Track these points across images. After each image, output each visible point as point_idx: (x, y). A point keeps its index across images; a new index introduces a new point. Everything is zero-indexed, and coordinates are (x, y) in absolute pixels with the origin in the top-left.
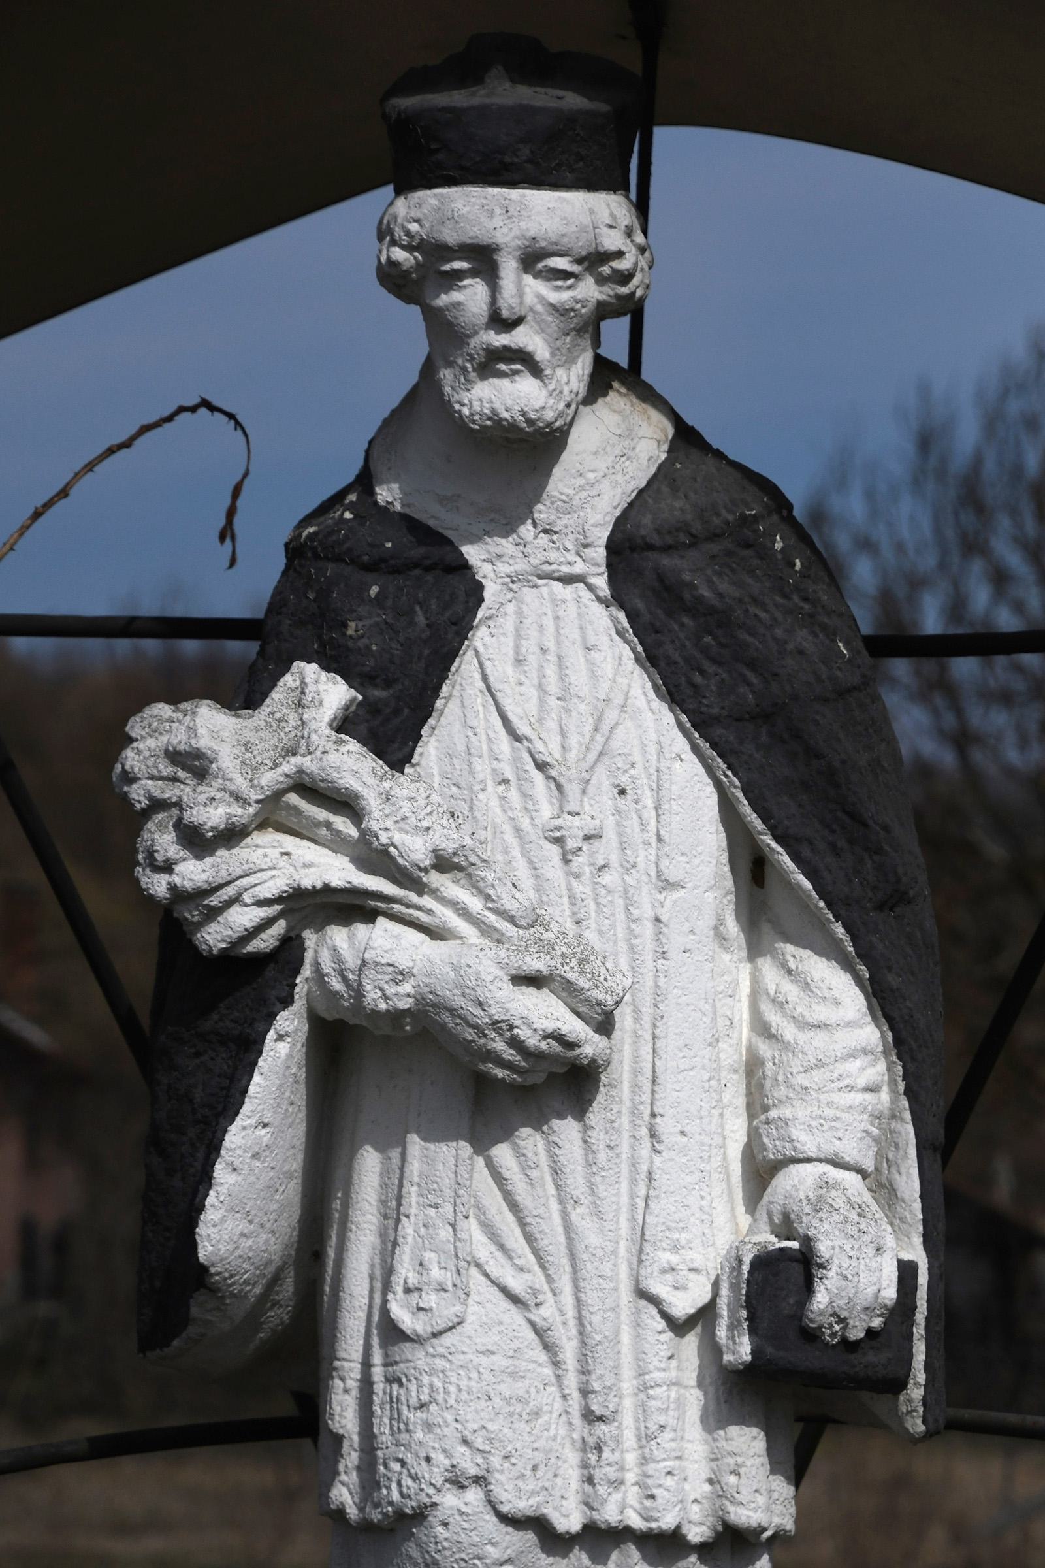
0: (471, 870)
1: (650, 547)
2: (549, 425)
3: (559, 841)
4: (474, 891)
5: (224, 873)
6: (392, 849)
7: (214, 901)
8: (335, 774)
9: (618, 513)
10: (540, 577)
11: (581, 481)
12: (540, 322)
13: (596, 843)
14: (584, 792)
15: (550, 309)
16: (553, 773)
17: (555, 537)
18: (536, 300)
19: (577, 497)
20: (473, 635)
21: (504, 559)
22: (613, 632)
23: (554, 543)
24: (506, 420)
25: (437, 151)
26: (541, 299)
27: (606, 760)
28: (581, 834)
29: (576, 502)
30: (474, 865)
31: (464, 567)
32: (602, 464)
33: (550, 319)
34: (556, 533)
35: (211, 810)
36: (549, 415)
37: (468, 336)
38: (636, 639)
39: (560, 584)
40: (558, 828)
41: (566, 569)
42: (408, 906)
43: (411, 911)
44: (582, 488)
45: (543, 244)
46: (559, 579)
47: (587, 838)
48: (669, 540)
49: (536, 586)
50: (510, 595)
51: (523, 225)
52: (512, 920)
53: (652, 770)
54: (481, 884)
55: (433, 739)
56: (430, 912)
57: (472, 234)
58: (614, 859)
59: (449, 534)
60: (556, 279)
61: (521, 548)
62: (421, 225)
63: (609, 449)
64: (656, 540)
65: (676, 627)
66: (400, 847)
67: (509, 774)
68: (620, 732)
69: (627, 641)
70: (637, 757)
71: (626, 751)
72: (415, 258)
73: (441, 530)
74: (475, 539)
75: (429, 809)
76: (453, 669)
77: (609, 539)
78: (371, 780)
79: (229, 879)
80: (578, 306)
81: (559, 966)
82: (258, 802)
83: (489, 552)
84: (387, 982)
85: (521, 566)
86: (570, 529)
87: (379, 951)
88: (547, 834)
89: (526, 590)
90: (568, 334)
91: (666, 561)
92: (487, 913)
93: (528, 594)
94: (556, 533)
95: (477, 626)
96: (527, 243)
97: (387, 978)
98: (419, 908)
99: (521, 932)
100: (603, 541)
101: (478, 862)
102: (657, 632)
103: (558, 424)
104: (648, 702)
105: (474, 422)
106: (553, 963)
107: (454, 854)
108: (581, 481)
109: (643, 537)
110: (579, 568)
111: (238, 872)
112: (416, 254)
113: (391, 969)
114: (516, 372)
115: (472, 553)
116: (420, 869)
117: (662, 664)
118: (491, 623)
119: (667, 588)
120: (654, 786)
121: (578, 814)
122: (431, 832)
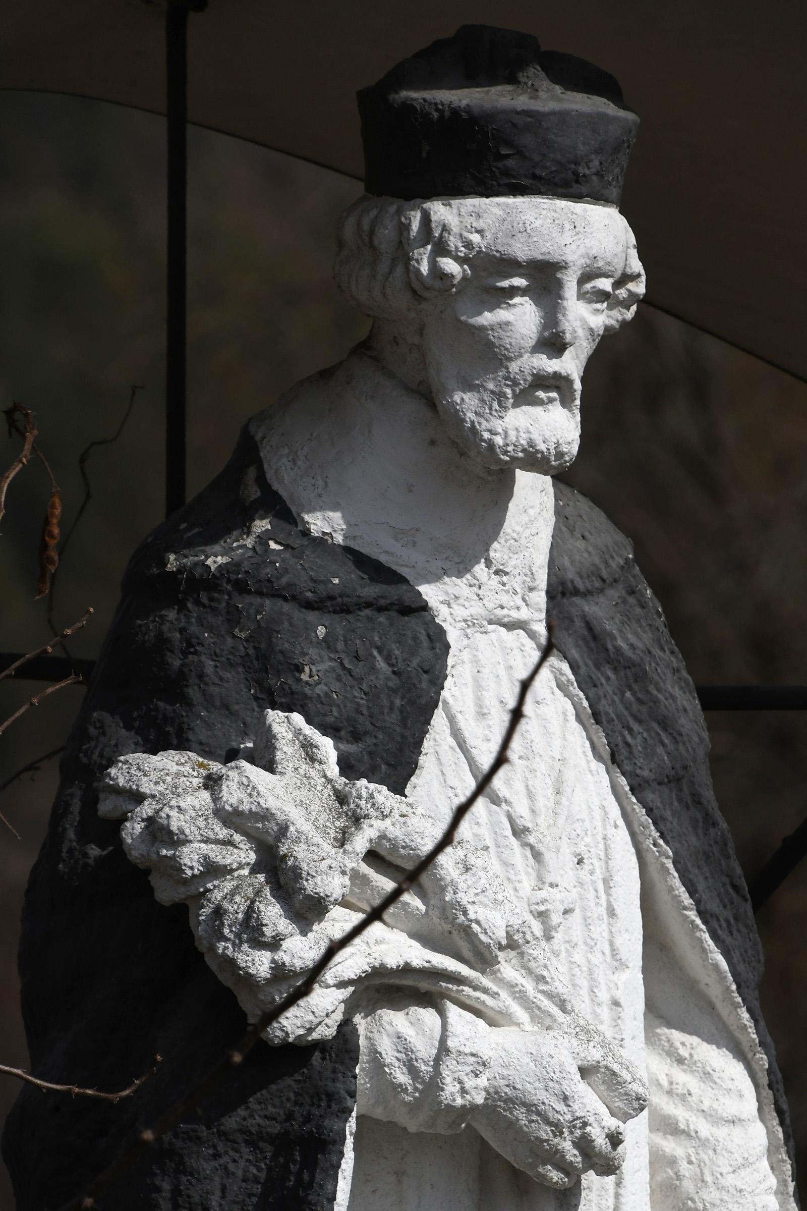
0: (525, 948)
4: (523, 972)
6: (474, 925)
8: (419, 840)
10: (491, 622)
15: (588, 333)
16: (531, 839)
17: (505, 579)
21: (461, 601)
22: (554, 684)
23: (504, 584)
24: (542, 452)
25: (507, 156)
26: (584, 321)
30: (528, 942)
31: (424, 607)
34: (506, 574)
37: (510, 359)
38: (581, 694)
43: (478, 994)
46: (504, 625)
53: (600, 838)
54: (533, 964)
56: (495, 995)
57: (544, 250)
59: (404, 571)
60: (597, 302)
61: (475, 589)
62: (482, 236)
66: (483, 923)
69: (568, 694)
72: (464, 270)
73: (394, 567)
74: (434, 577)
83: (447, 593)
84: (467, 1074)
85: (476, 609)
86: (518, 571)
87: (463, 1041)
88: (533, 907)
89: (478, 635)
92: (540, 996)
94: (506, 574)
96: (588, 262)
97: (468, 1069)
98: (485, 991)
104: (588, 762)
105: (506, 453)
110: (524, 614)
112: (466, 267)
113: (473, 1059)
114: (551, 401)
115: (430, 593)
119: (595, 638)
120: (603, 856)
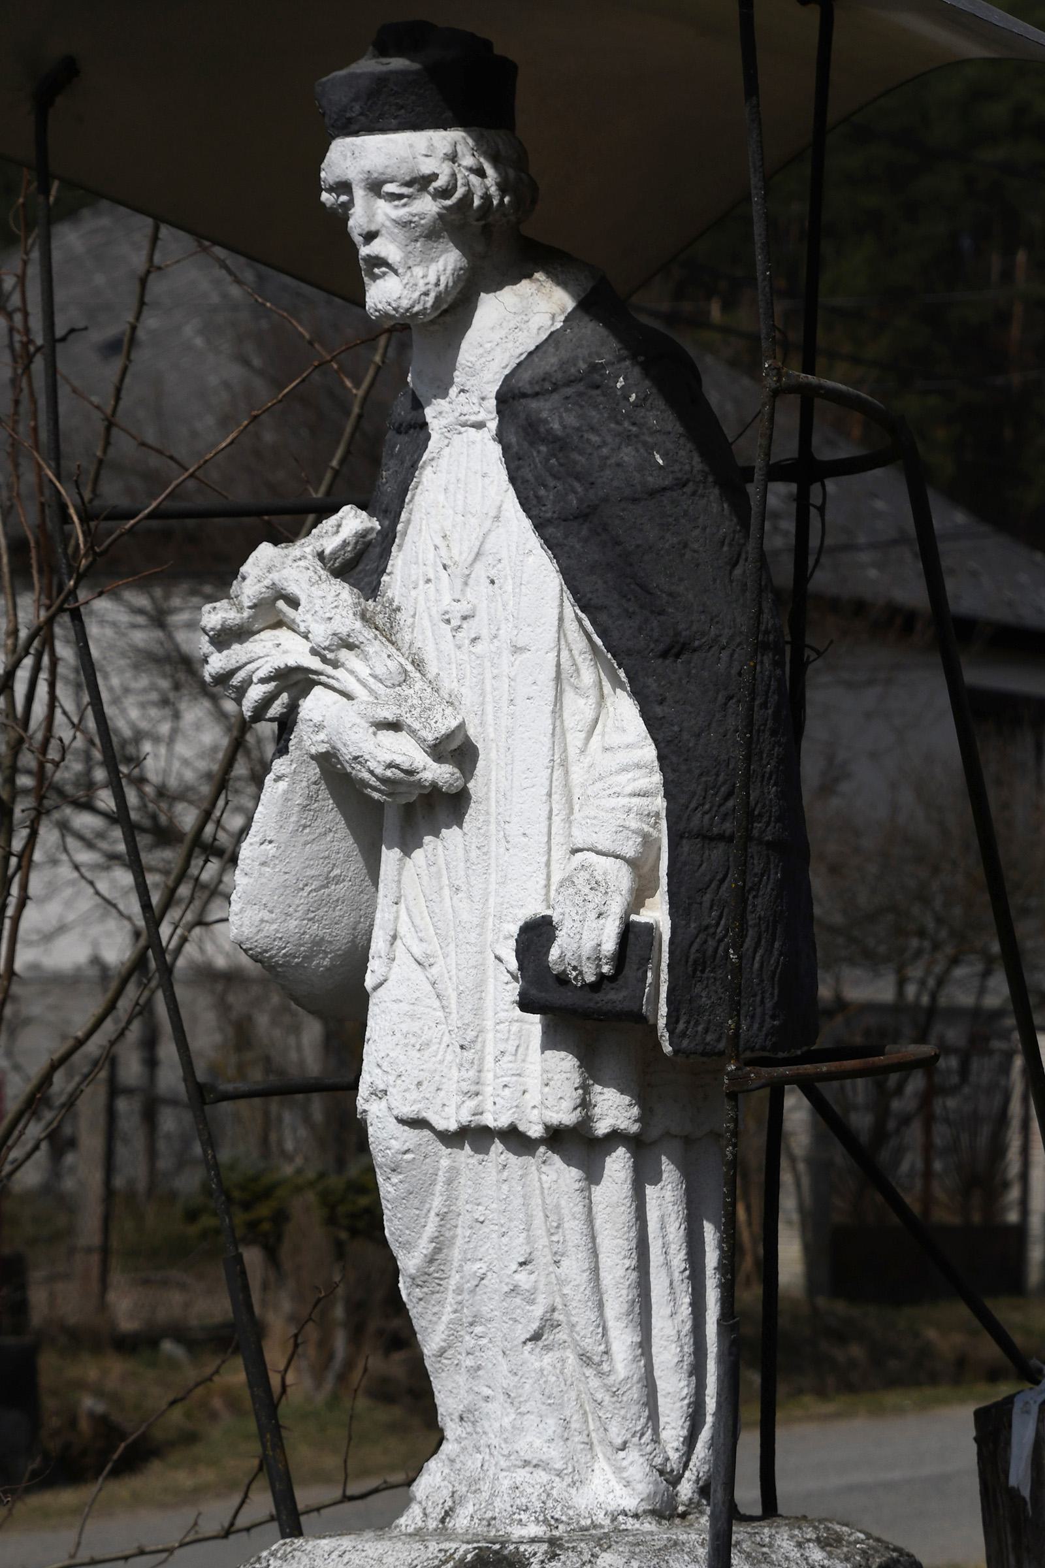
1: (524, 395)
2: (407, 310)
3: (448, 621)
5: (233, 661)
7: (236, 681)
9: (507, 371)
10: (463, 426)
11: (481, 351)
12: (391, 234)
13: (471, 621)
14: (466, 584)
18: (385, 218)
19: (478, 363)
20: (421, 474)
27: (483, 559)
28: (459, 615)
29: (478, 367)
32: (496, 336)
33: (396, 231)
35: (212, 616)
36: (405, 303)
39: (474, 430)
40: (446, 613)
41: (473, 418)
42: (328, 677)
44: (482, 356)
45: (375, 175)
47: (465, 618)
48: (537, 388)
49: (460, 433)
50: (446, 441)
51: (362, 163)
52: (381, 681)
55: (401, 555)
58: (485, 633)
63: (505, 324)
64: (529, 391)
65: (535, 454)
67: (431, 576)
68: (492, 538)
70: (504, 554)
71: (495, 551)
75: (336, 604)
76: (407, 500)
77: (498, 393)
78: (305, 586)
79: (238, 665)
80: (416, 219)
81: (403, 714)
82: (250, 608)
89: (456, 436)
90: (416, 241)
91: (534, 404)
93: (456, 438)
95: (422, 467)
99: (388, 690)
100: (494, 394)
101: (365, 641)
102: (520, 459)
103: (416, 309)
106: (398, 712)
107: (349, 635)
108: (481, 351)
109: (519, 388)
111: (244, 660)
114: (384, 274)
116: (324, 649)
117: (519, 483)
118: (434, 463)
121: (459, 601)
122: (333, 621)
